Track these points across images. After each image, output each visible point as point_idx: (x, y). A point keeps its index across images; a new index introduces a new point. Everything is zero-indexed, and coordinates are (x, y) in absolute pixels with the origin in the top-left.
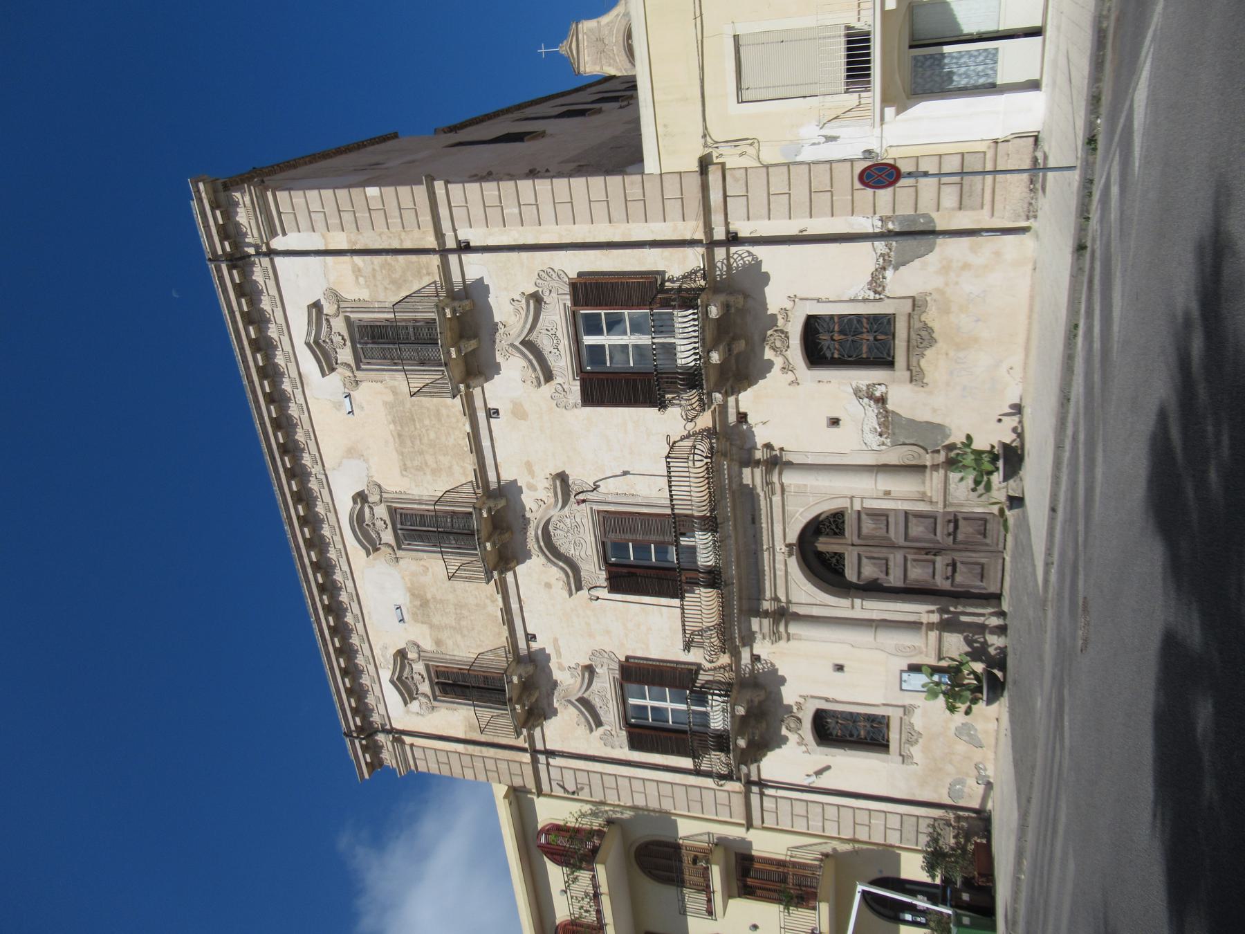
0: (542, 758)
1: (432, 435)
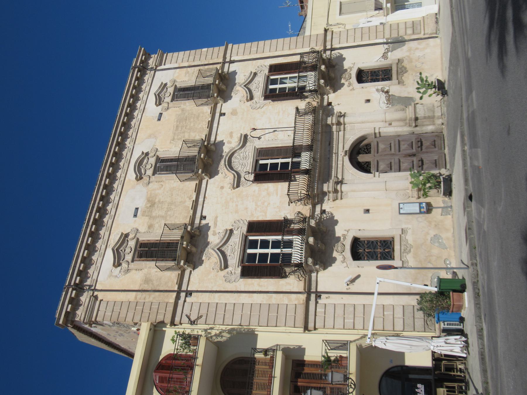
0: (183, 295)
1: (192, 125)
